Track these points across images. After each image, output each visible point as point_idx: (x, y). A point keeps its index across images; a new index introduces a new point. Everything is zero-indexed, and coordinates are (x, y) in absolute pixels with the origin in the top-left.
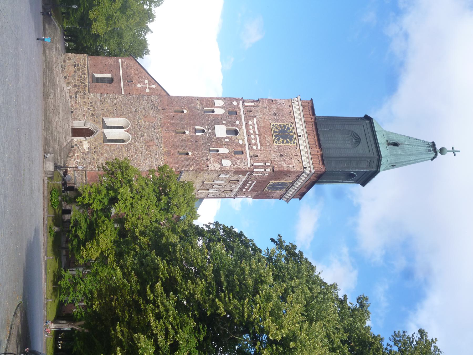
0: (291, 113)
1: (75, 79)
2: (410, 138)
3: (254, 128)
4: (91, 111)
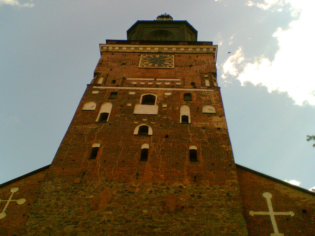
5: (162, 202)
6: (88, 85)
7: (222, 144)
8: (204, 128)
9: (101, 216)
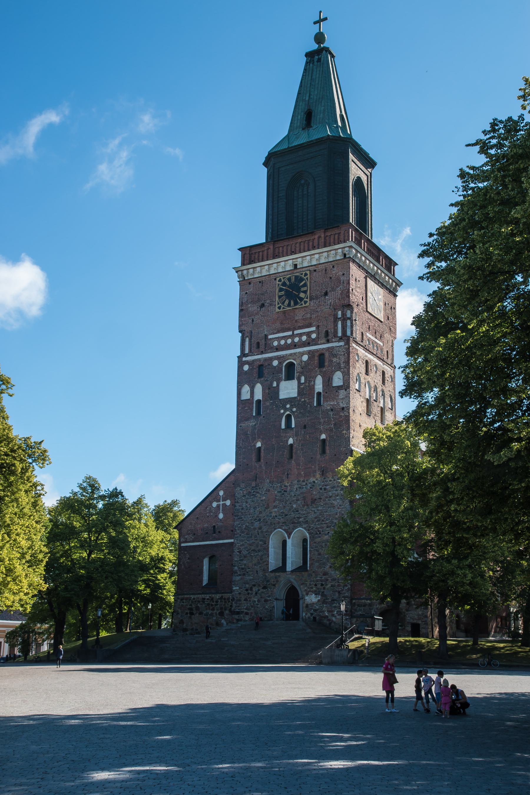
0: (261, 281)
1: (212, 614)
2: (299, 94)
3: (283, 338)
4: (259, 590)
5: (304, 497)
6: (238, 357)
7: (343, 430)
8: (332, 410)
9: (271, 513)
